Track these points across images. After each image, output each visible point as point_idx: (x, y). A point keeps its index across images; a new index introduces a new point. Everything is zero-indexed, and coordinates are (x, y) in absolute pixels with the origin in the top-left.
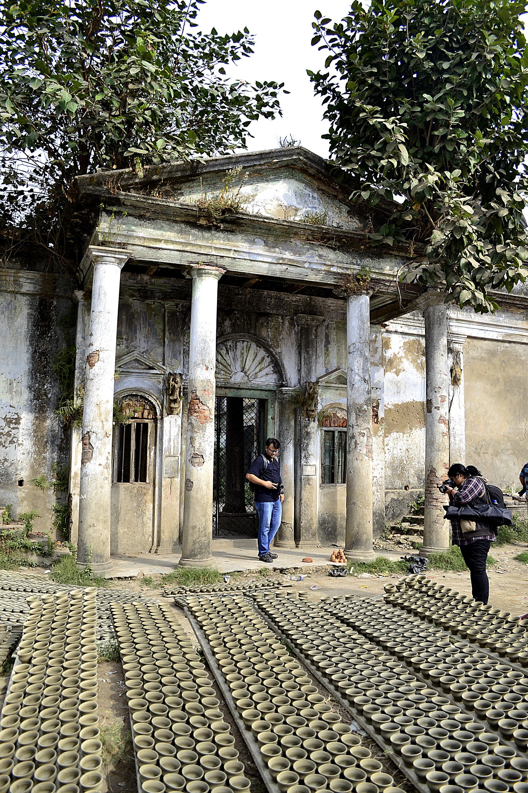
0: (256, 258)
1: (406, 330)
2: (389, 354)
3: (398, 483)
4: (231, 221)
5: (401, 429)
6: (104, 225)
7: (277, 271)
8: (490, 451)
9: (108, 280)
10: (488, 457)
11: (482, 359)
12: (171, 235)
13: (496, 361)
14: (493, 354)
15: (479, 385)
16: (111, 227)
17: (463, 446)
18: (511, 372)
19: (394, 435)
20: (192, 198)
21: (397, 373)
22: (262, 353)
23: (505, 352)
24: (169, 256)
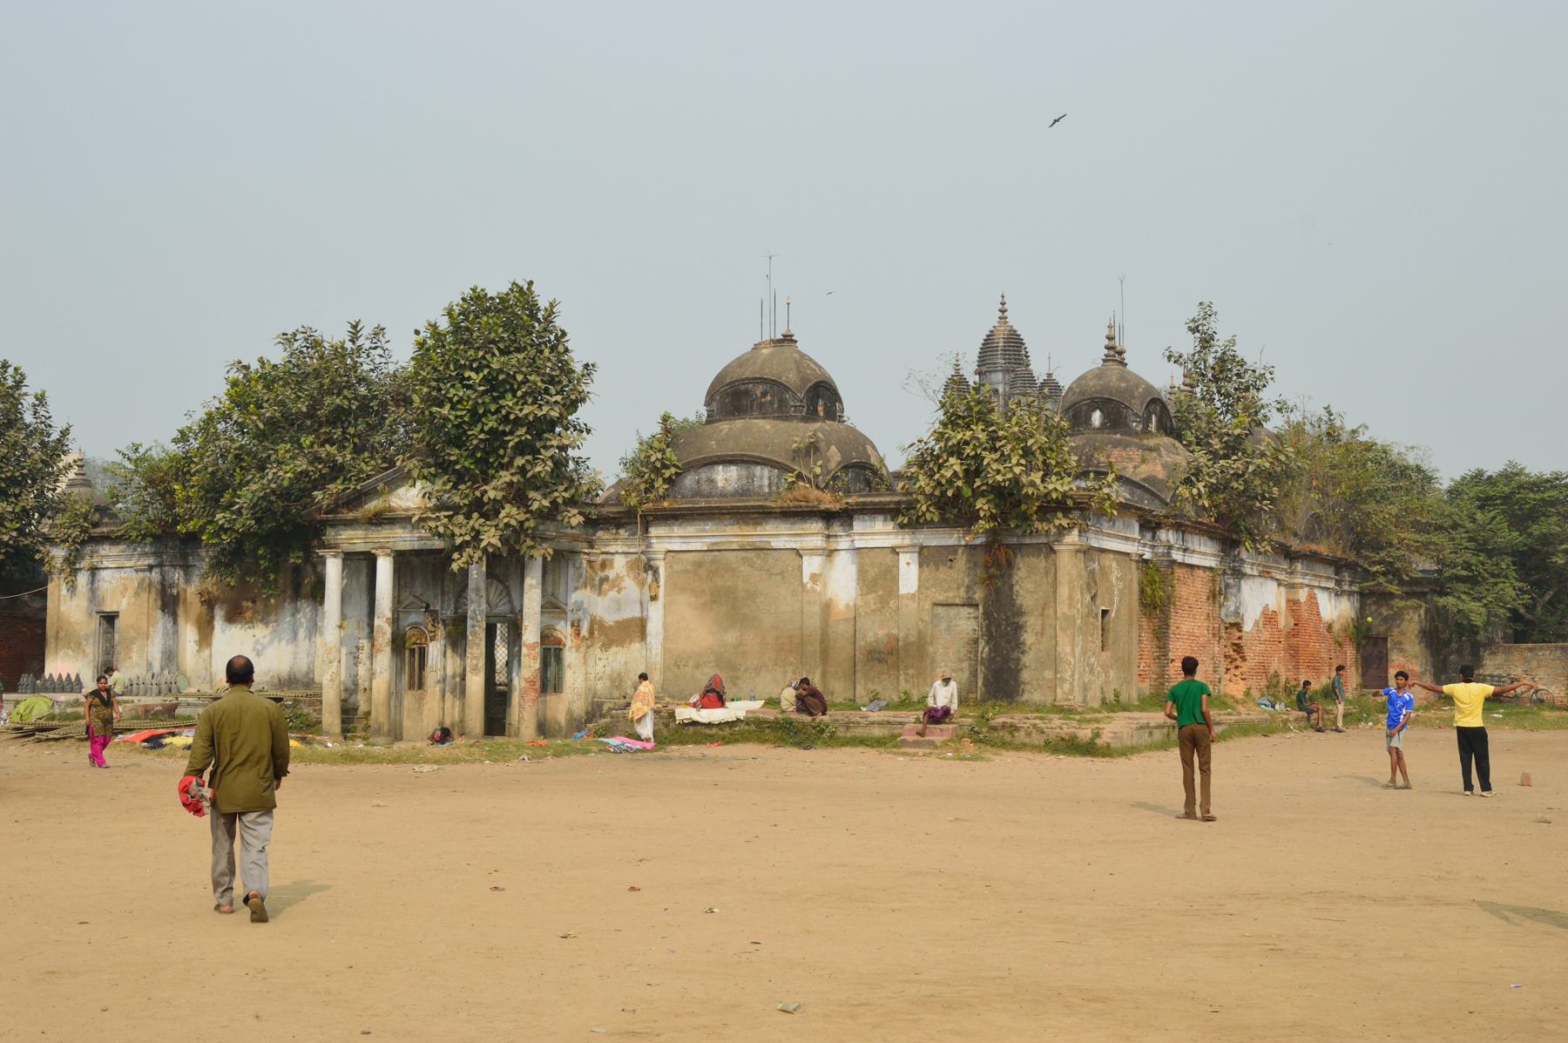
0: (405, 539)
1: (626, 549)
2: (611, 574)
3: (616, 694)
4: (381, 519)
5: (621, 643)
6: (330, 535)
7: (416, 545)
8: (691, 663)
9: (333, 569)
10: (688, 670)
11: (687, 571)
12: (360, 533)
13: (702, 572)
14: (700, 564)
15: (683, 600)
16: (75, 644)
17: (659, 659)
18: (719, 581)
19: (614, 649)
20: (373, 505)
21: (619, 591)
22: (501, 587)
23: (713, 561)
24: (361, 547)
